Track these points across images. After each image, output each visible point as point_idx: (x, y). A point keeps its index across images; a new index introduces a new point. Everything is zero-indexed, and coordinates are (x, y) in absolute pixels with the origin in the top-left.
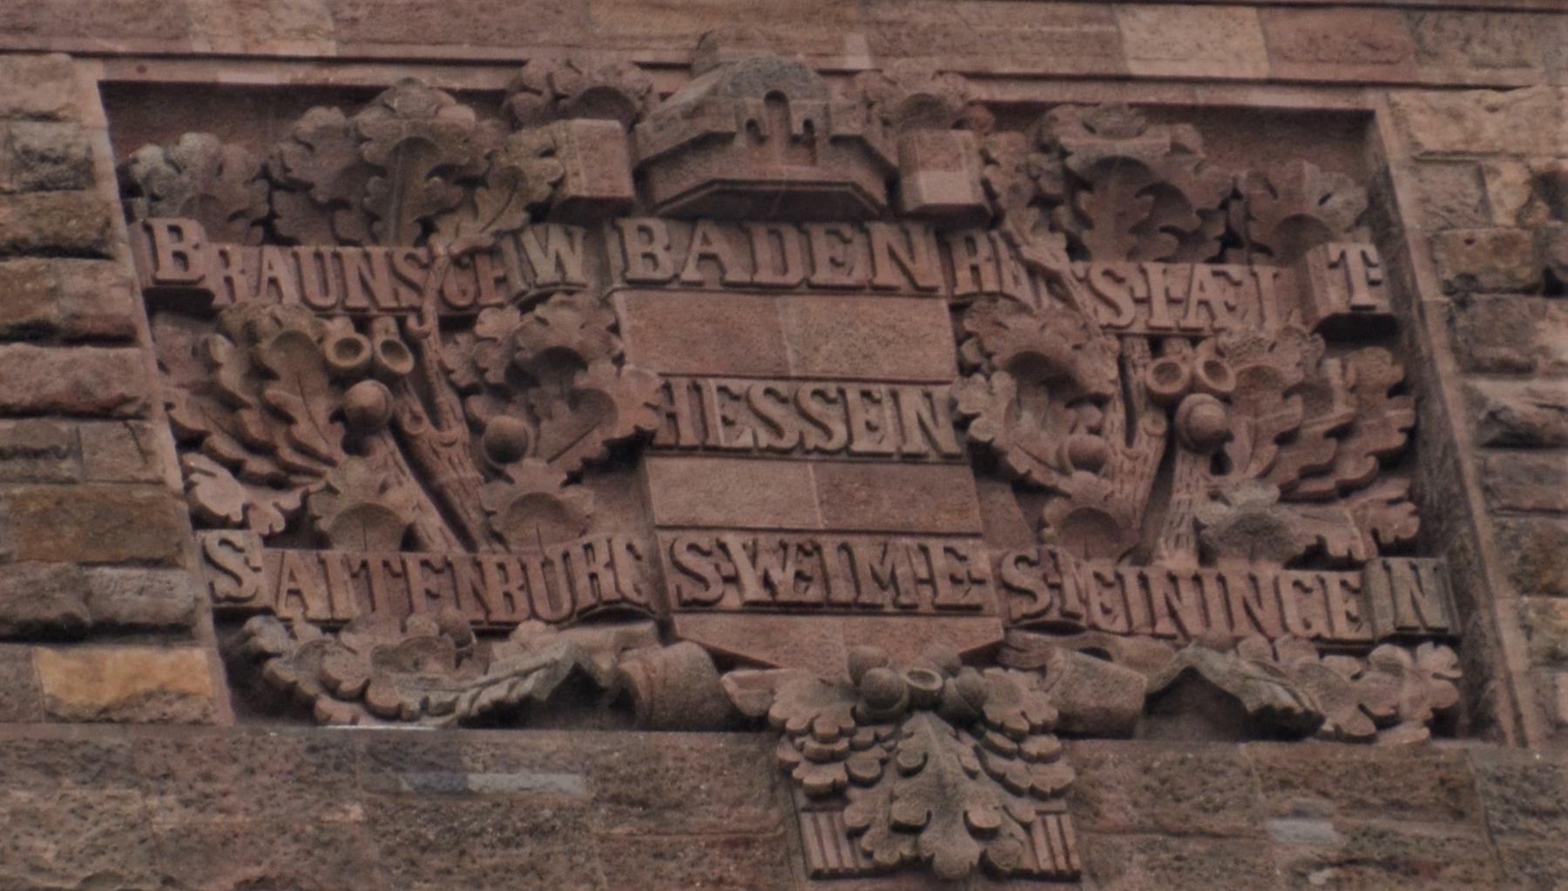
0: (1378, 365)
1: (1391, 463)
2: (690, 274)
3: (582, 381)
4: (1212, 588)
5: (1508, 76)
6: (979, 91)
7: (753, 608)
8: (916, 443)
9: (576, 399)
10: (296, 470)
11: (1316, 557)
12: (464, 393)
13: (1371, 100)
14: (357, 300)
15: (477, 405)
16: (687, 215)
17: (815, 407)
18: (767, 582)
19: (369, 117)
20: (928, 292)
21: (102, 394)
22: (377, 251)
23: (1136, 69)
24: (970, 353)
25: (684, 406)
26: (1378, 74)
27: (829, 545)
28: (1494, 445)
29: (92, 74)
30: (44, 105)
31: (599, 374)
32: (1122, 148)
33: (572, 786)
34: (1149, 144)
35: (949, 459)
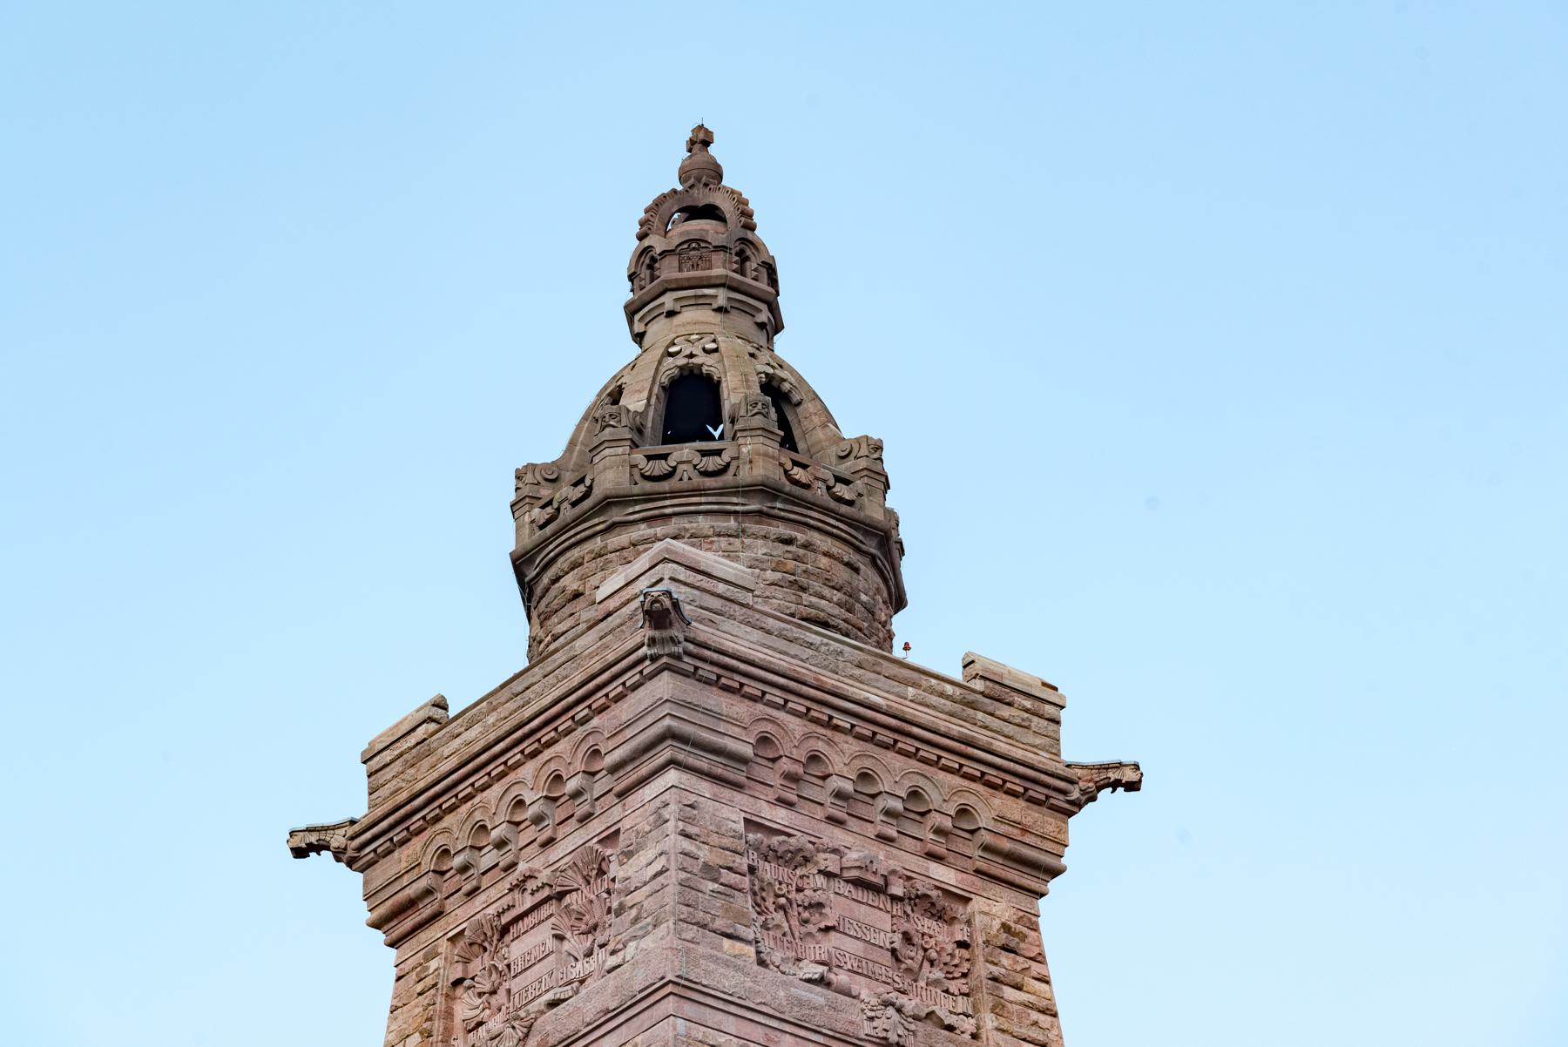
0: (965, 953)
1: (964, 975)
2: (846, 894)
3: (824, 911)
4: (929, 992)
5: (998, 899)
6: (905, 872)
7: (849, 970)
8: (882, 944)
9: (821, 914)
10: (763, 911)
11: (947, 991)
12: (799, 906)
13: (972, 896)
14: (781, 879)
15: (801, 909)
16: (847, 881)
17: (865, 930)
18: (852, 966)
19: (792, 840)
20: (888, 912)
21: (740, 887)
22: (786, 870)
23: (932, 876)
24: (895, 927)
25: (841, 922)
26: (975, 891)
27: (864, 961)
28: (990, 979)
29: (743, 815)
30: (734, 819)
31: (826, 910)
32: (929, 893)
33: (822, 1000)
34: (934, 893)
35: (888, 950)
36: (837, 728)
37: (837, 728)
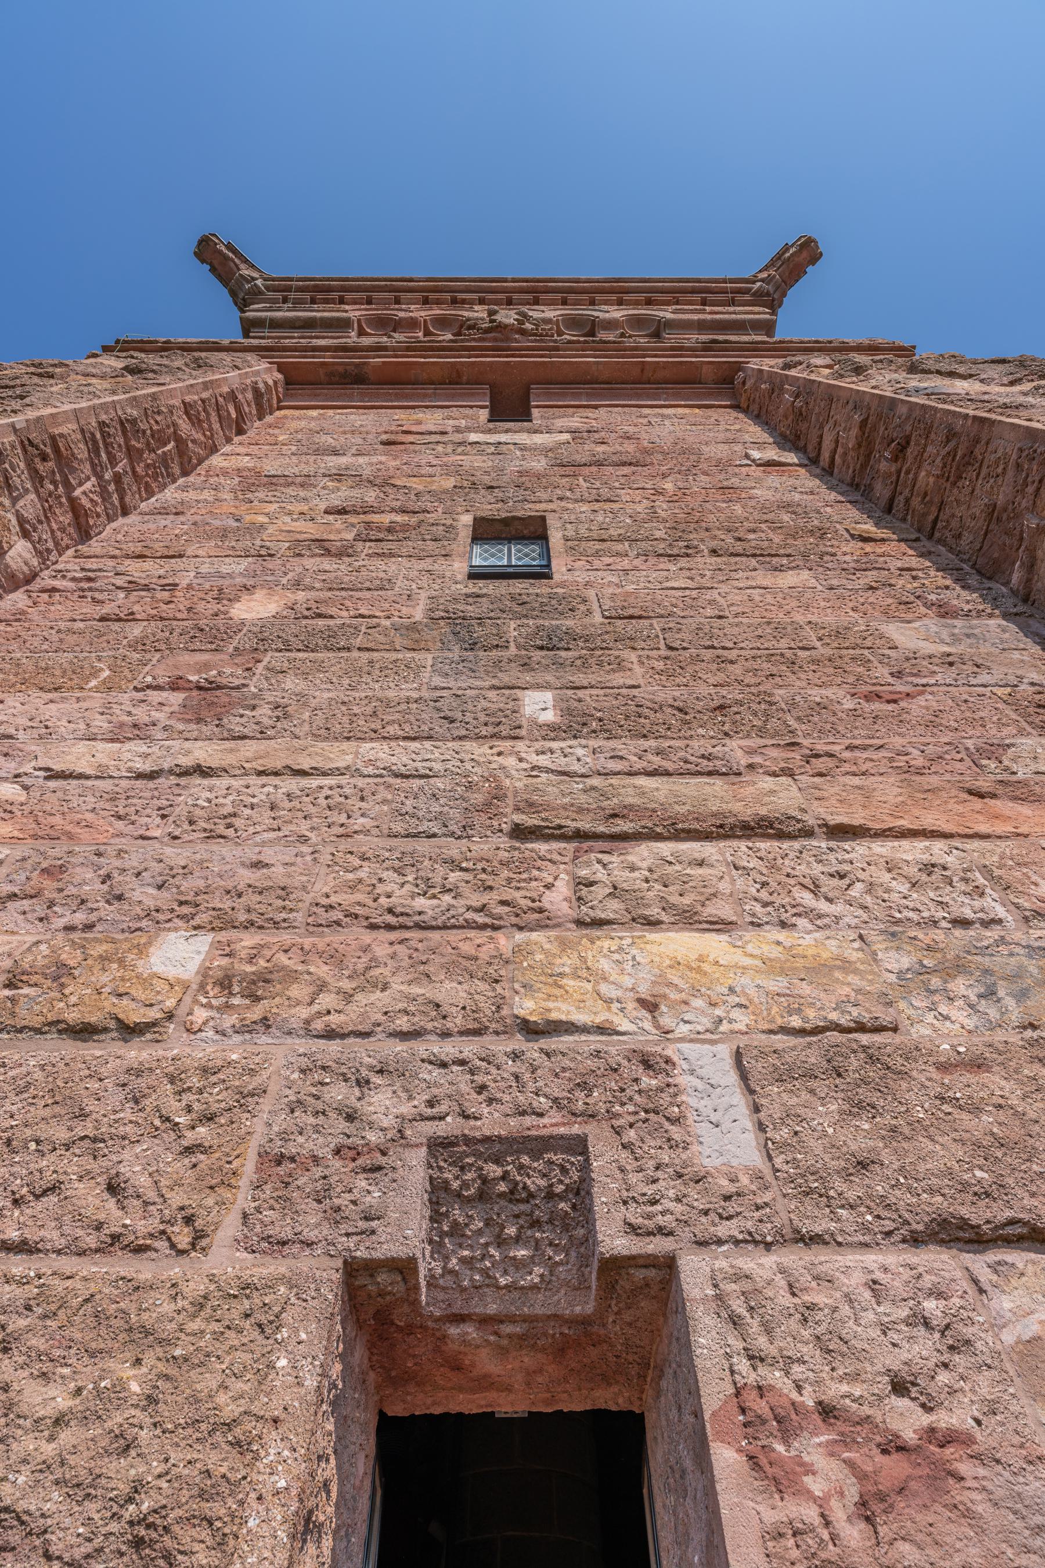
36: (463, 301)
37: (463, 301)
